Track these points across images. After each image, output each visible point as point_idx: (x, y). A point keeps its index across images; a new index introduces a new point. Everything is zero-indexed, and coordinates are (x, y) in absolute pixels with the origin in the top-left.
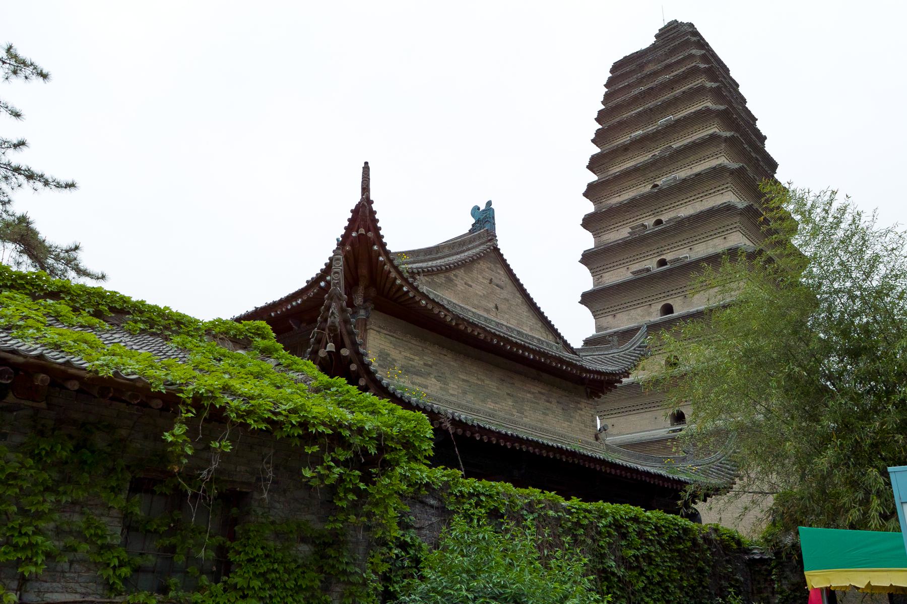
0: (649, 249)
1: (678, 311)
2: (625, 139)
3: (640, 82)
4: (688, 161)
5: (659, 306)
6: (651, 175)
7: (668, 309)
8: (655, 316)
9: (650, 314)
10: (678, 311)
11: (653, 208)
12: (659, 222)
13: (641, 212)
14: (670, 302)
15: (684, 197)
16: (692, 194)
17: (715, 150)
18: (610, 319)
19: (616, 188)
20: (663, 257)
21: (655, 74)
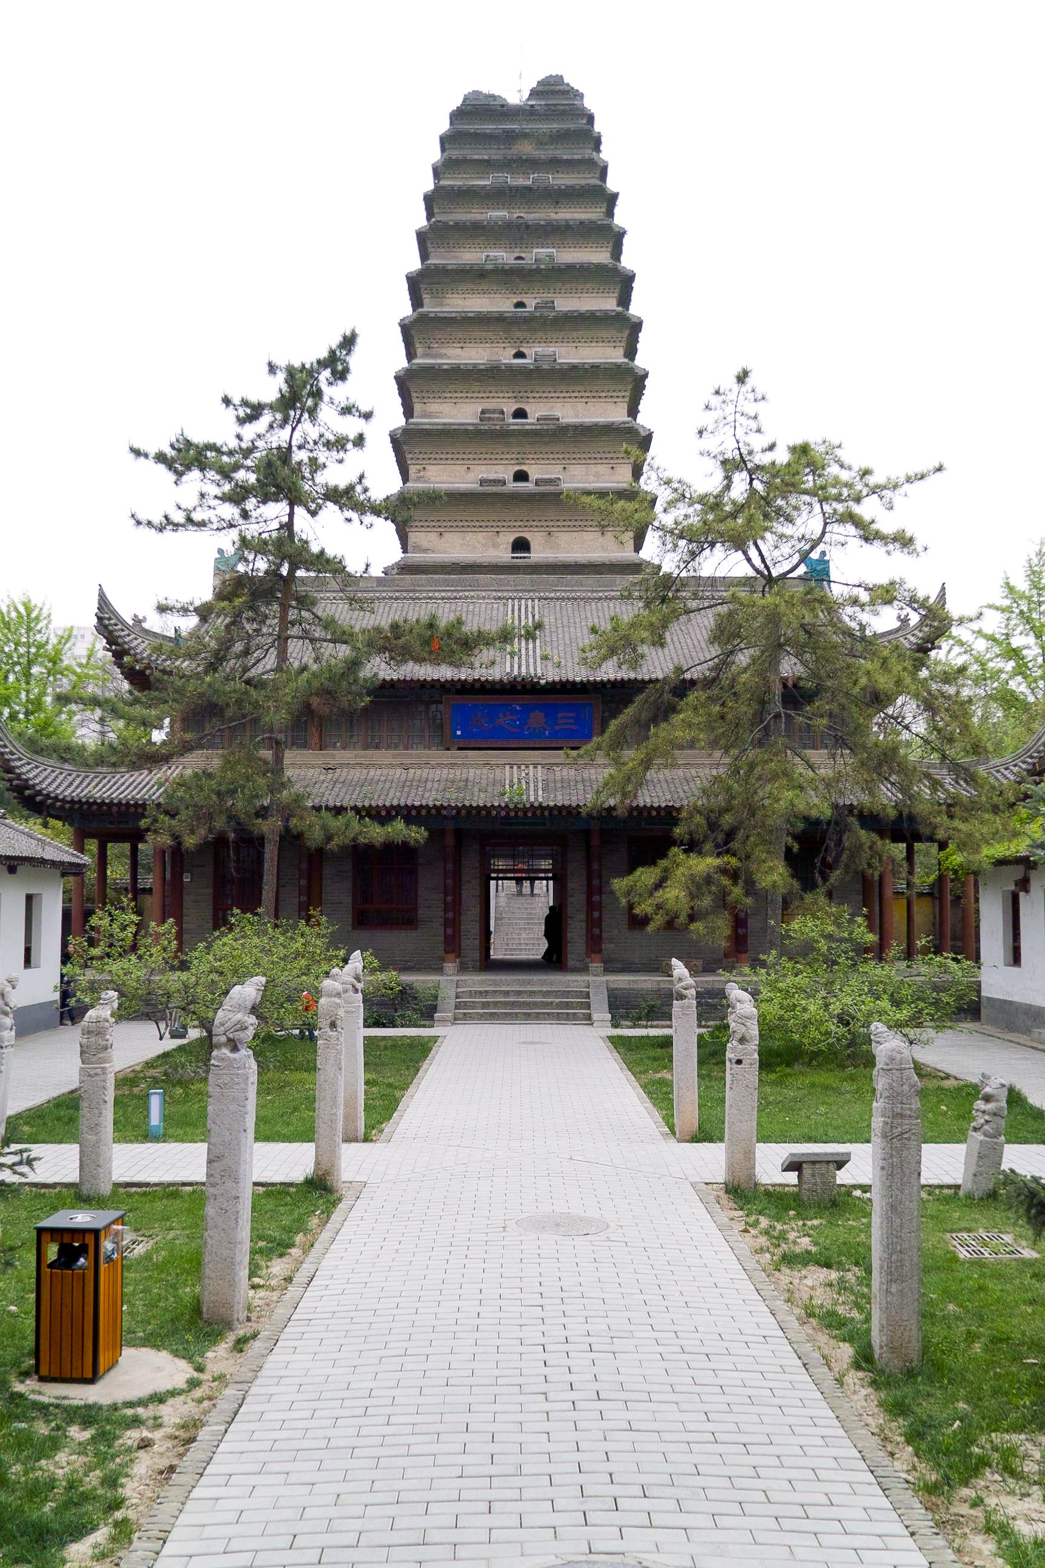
0: (506, 450)
1: (539, 554)
2: (472, 255)
3: (507, 165)
4: (575, 334)
5: (511, 538)
6: (519, 334)
7: (521, 545)
8: (503, 554)
9: (495, 545)
10: (539, 554)
11: (517, 388)
12: (520, 414)
13: (499, 388)
14: (527, 535)
15: (564, 388)
16: (576, 388)
17: (613, 333)
18: (433, 536)
19: (460, 335)
20: (524, 468)
21: (533, 164)
